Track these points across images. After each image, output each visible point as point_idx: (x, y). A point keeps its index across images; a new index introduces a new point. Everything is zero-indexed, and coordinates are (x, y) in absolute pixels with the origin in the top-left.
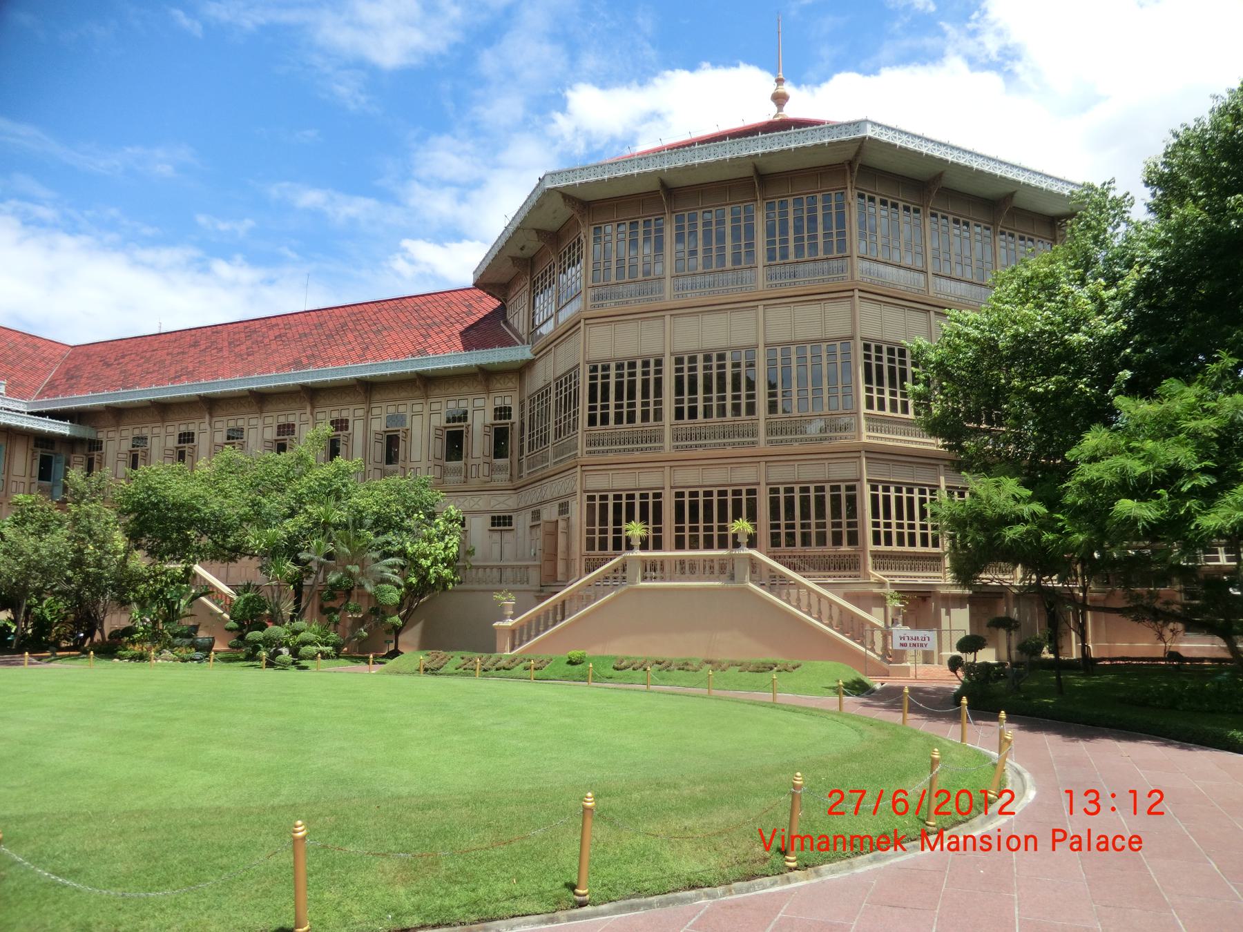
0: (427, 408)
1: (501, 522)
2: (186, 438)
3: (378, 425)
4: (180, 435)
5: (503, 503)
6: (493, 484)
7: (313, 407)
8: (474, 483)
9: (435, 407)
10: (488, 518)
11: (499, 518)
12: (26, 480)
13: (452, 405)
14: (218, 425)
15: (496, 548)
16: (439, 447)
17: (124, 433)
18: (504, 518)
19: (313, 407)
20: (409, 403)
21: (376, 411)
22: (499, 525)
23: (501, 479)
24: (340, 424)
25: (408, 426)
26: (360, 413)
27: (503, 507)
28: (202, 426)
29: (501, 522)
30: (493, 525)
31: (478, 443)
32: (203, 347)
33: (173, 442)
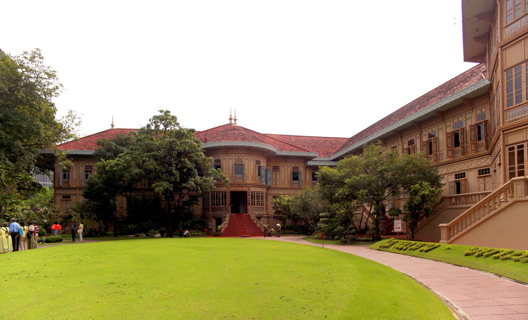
0: (444, 125)
1: (484, 172)
3: (425, 139)
5: (484, 162)
6: (478, 153)
7: (402, 138)
8: (471, 154)
9: (448, 124)
10: (476, 171)
11: (483, 170)
13: (455, 121)
15: (482, 186)
16: (452, 141)
18: (486, 170)
19: (402, 138)
20: (436, 125)
21: (424, 133)
22: (483, 174)
23: (483, 150)
24: (411, 143)
25: (437, 136)
26: (418, 135)
27: (484, 164)
29: (484, 172)
30: (480, 174)
31: (470, 135)
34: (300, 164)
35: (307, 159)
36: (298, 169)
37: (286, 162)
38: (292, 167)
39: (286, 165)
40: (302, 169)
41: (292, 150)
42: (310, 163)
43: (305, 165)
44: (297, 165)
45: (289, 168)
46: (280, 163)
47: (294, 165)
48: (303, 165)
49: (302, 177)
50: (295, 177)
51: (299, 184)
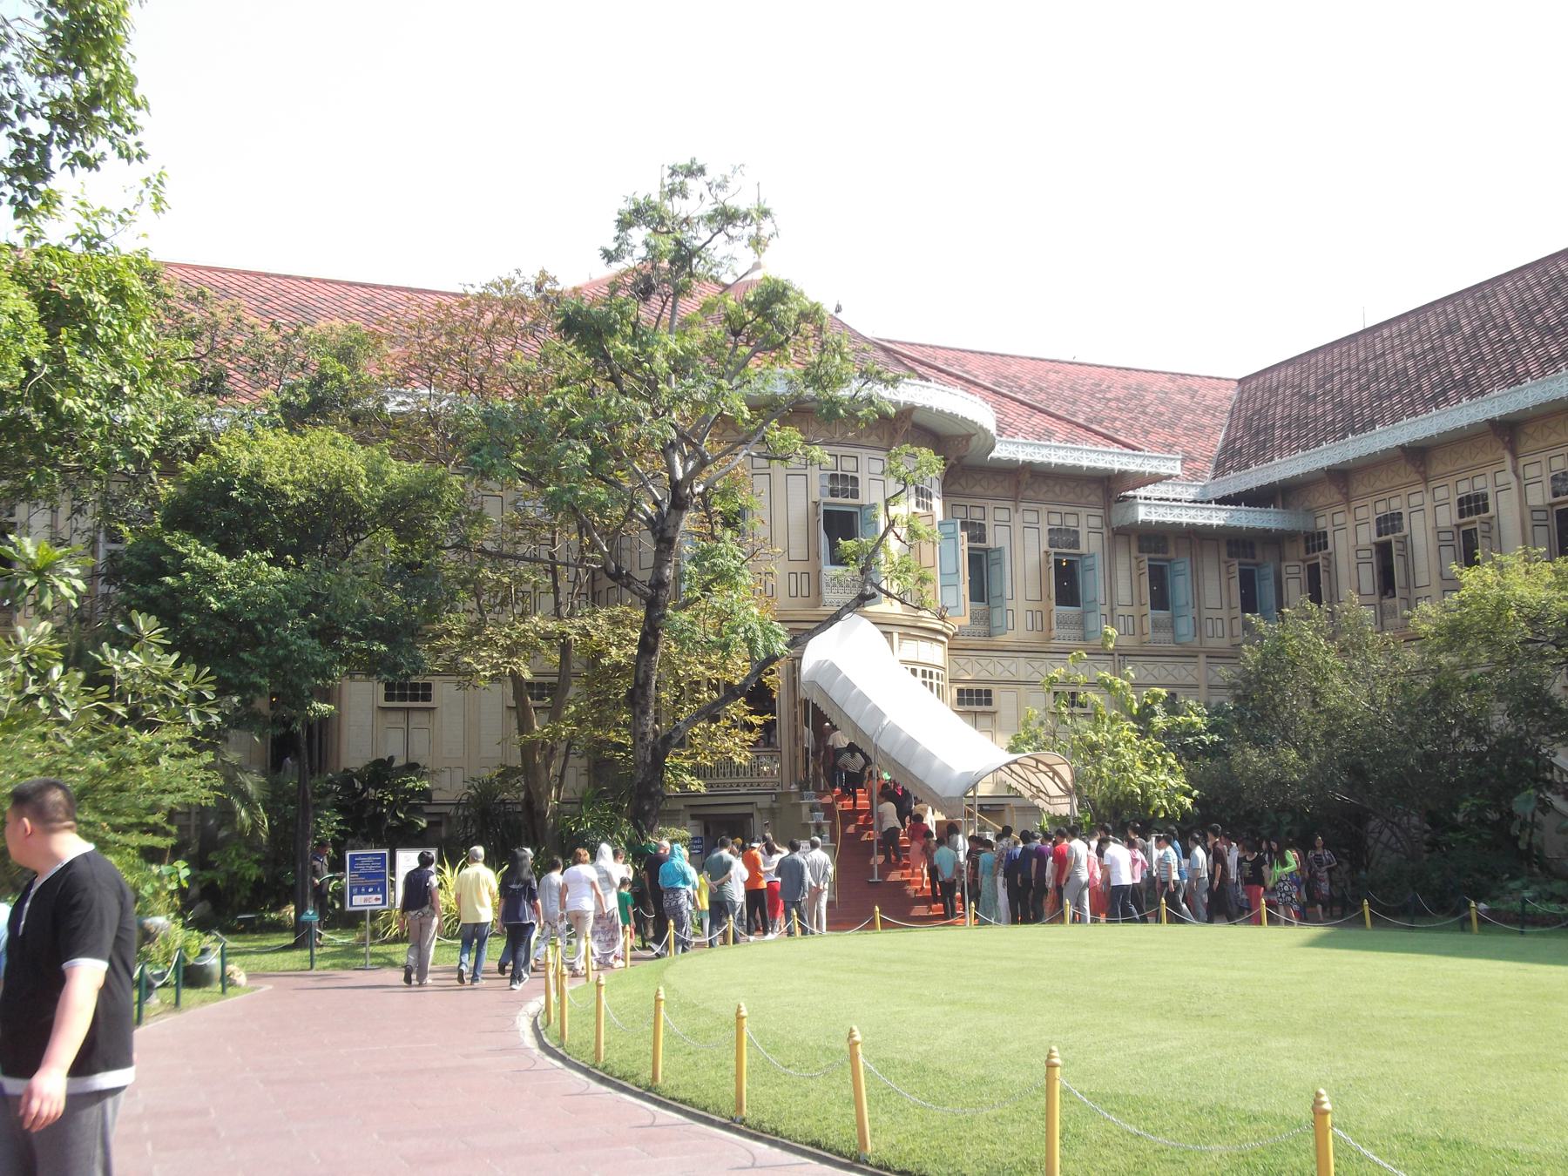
2: (1473, 504)
4: (1461, 502)
12: (1223, 614)
14: (1532, 471)
17: (1441, 493)
28: (1501, 478)
32: (1467, 330)
33: (1448, 516)
34: (1083, 512)
35: (1109, 488)
36: (1076, 544)
37: (1015, 499)
38: (1045, 528)
39: (1017, 517)
40: (1091, 543)
41: (1049, 434)
42: (1143, 514)
43: (1107, 521)
44: (1071, 522)
45: (1031, 534)
46: (990, 505)
47: (1056, 520)
48: (1095, 522)
49: (1093, 584)
50: (1067, 583)
51: (1082, 623)
